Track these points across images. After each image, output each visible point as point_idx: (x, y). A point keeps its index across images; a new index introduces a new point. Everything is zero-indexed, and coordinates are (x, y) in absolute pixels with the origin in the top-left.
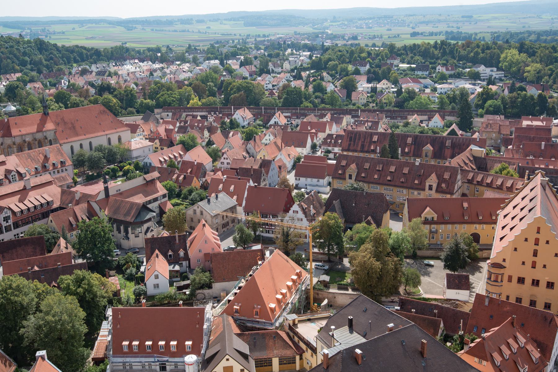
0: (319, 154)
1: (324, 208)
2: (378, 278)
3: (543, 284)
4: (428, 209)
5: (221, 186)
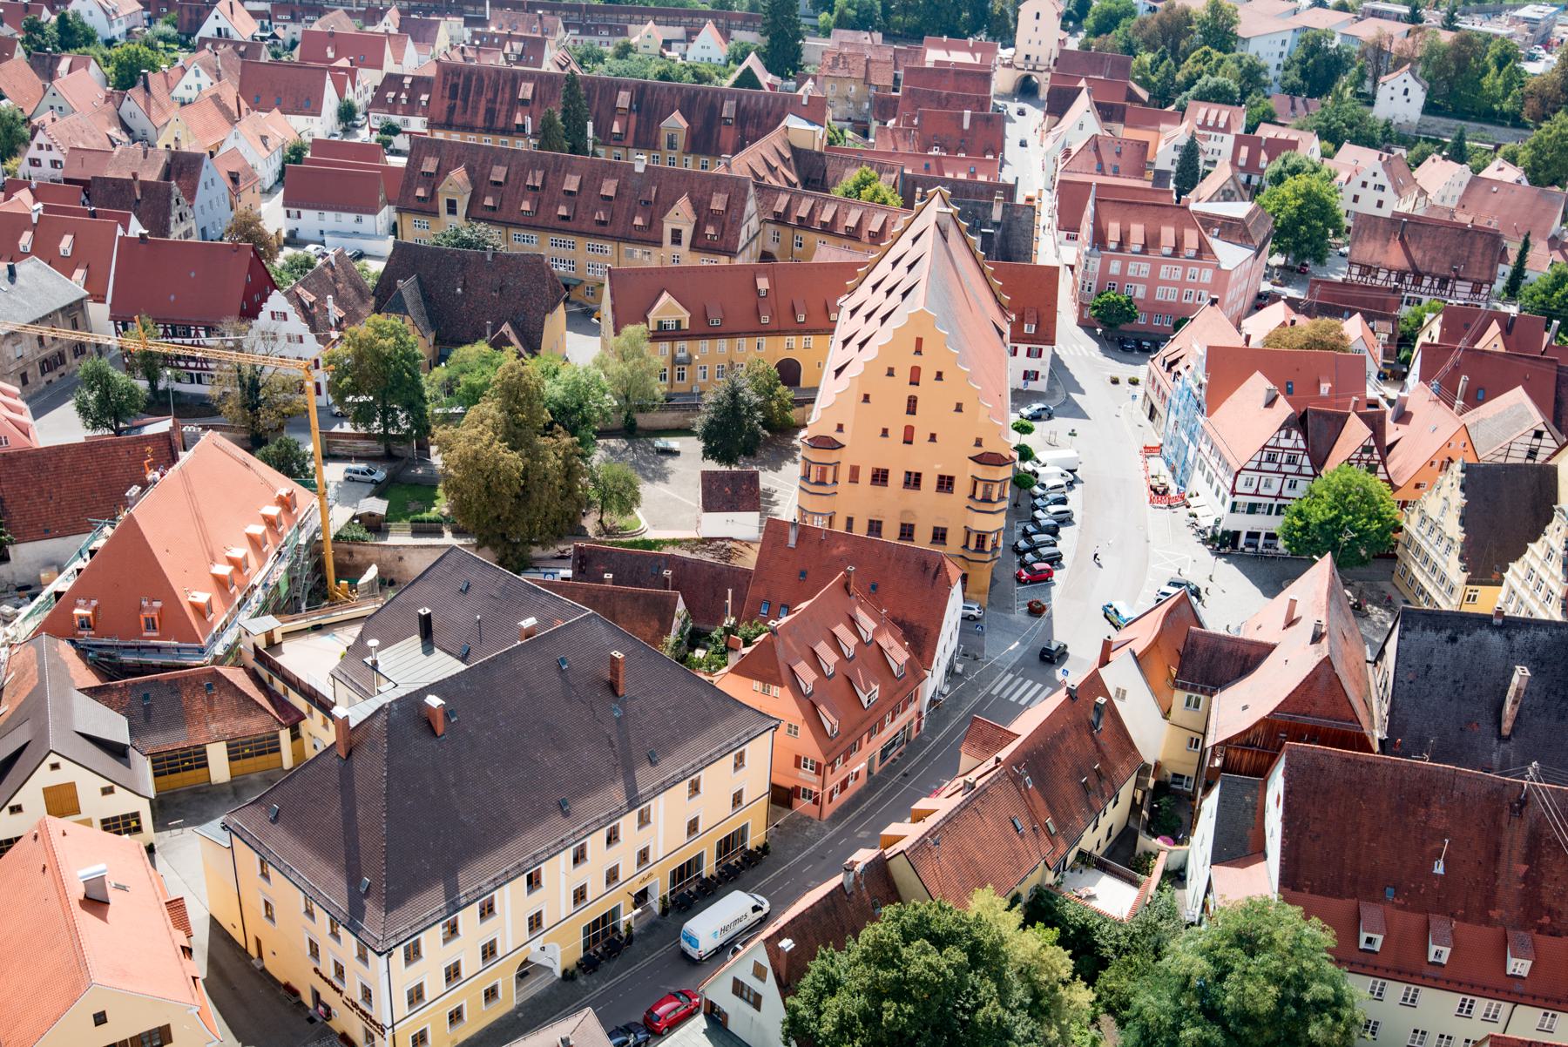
0: (363, 136)
1: (372, 301)
2: (517, 496)
3: (929, 482)
4: (666, 296)
5: (26, 240)
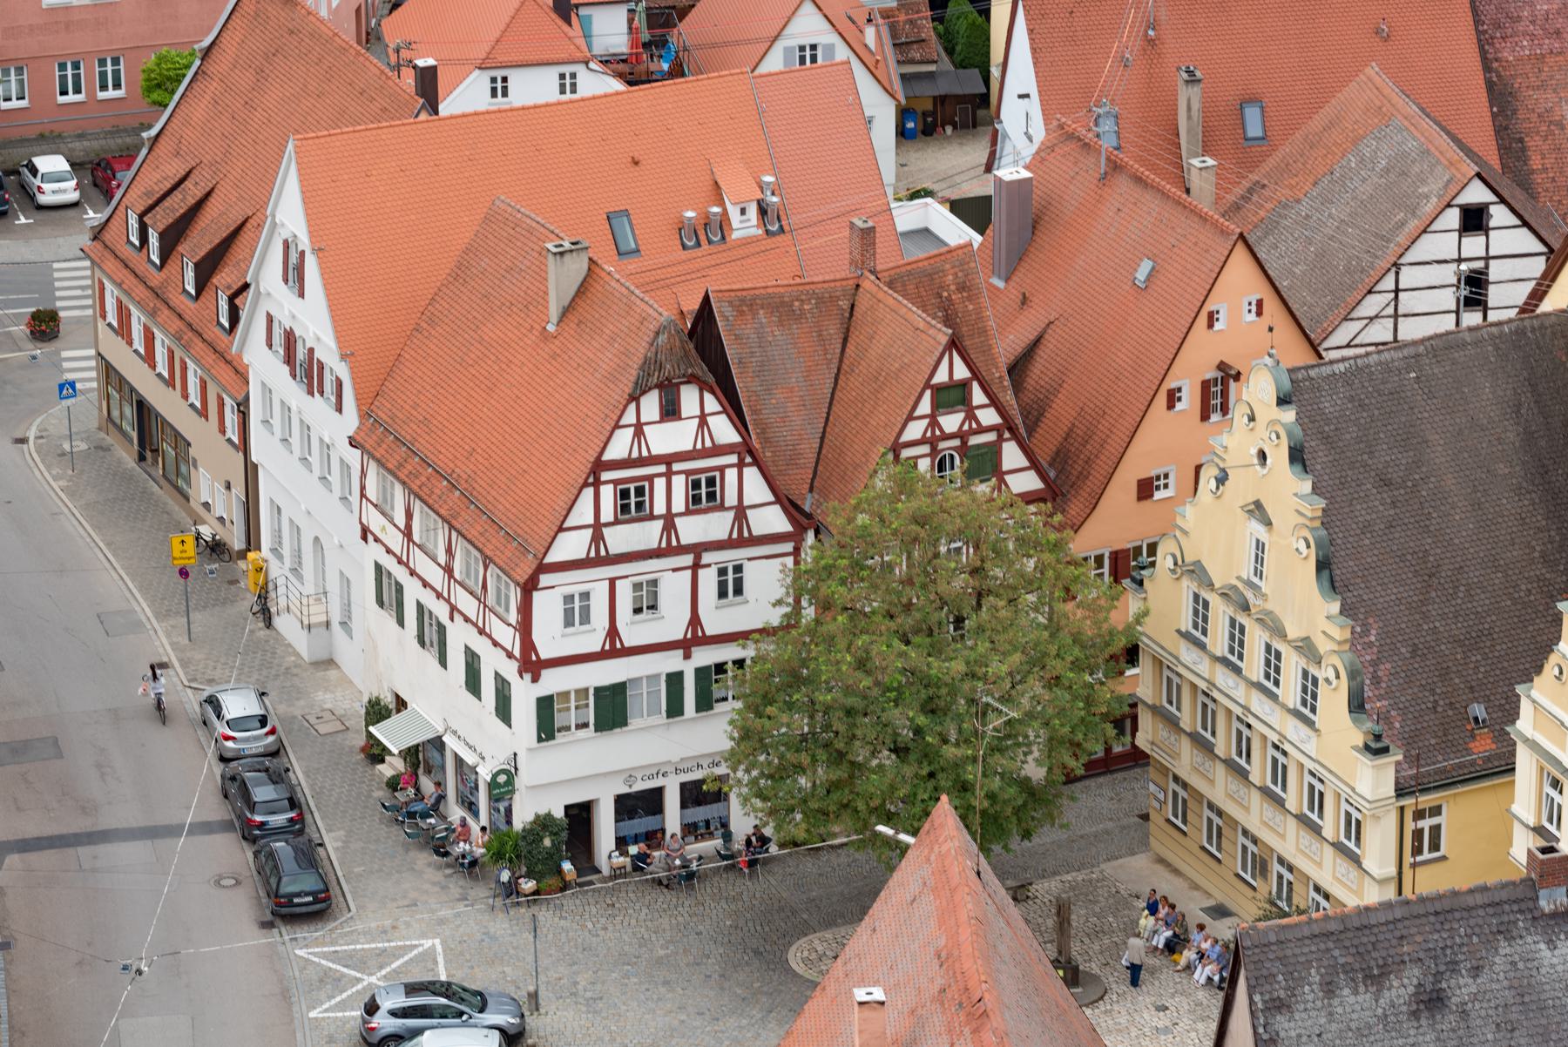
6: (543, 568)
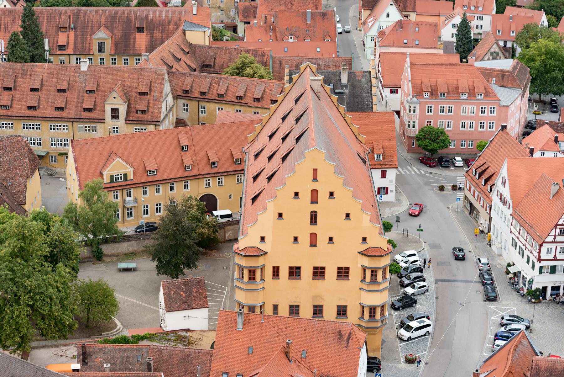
3: (331, 273)
6: (544, 242)
